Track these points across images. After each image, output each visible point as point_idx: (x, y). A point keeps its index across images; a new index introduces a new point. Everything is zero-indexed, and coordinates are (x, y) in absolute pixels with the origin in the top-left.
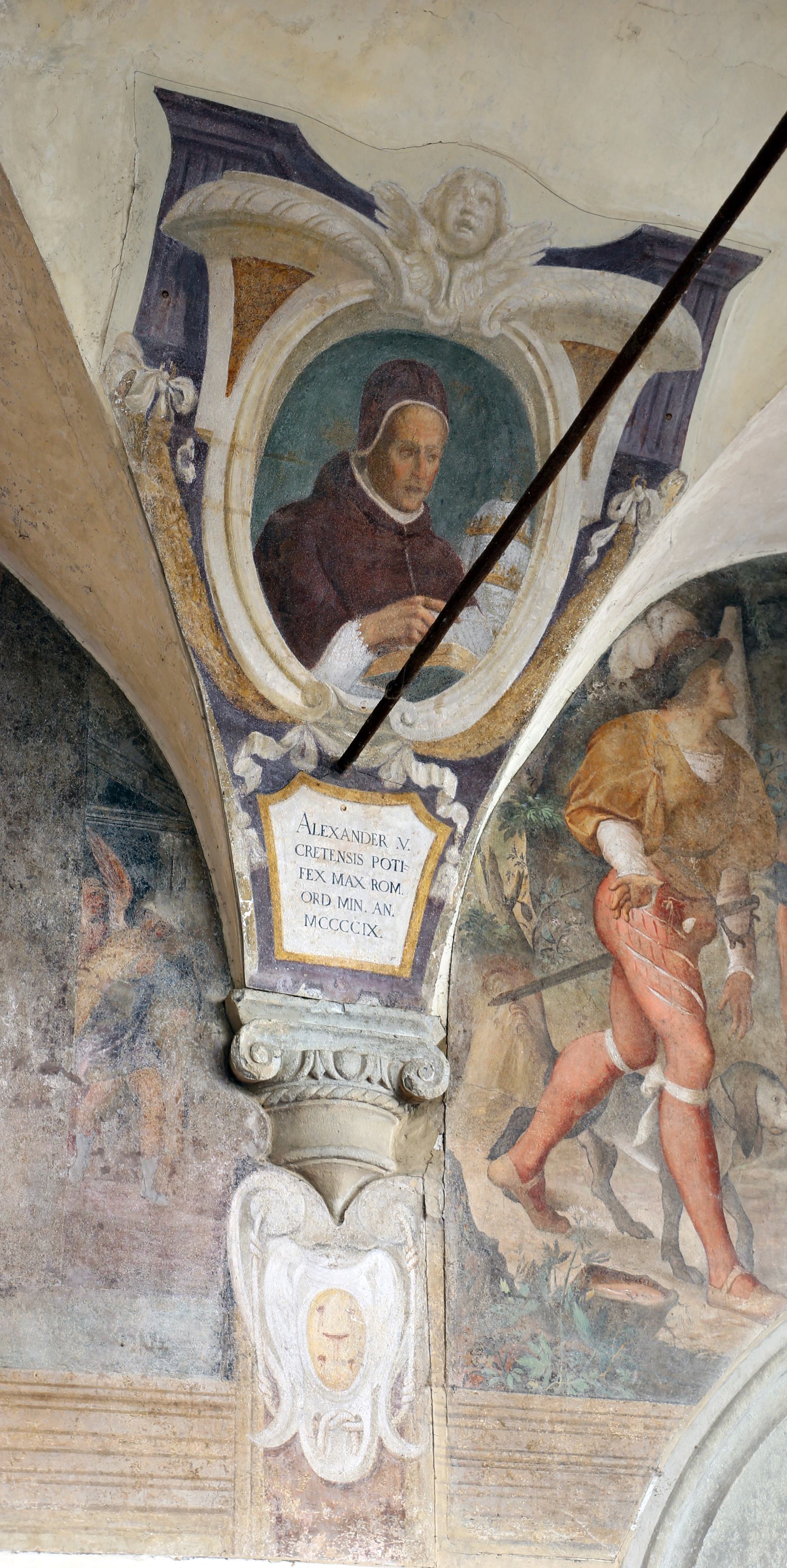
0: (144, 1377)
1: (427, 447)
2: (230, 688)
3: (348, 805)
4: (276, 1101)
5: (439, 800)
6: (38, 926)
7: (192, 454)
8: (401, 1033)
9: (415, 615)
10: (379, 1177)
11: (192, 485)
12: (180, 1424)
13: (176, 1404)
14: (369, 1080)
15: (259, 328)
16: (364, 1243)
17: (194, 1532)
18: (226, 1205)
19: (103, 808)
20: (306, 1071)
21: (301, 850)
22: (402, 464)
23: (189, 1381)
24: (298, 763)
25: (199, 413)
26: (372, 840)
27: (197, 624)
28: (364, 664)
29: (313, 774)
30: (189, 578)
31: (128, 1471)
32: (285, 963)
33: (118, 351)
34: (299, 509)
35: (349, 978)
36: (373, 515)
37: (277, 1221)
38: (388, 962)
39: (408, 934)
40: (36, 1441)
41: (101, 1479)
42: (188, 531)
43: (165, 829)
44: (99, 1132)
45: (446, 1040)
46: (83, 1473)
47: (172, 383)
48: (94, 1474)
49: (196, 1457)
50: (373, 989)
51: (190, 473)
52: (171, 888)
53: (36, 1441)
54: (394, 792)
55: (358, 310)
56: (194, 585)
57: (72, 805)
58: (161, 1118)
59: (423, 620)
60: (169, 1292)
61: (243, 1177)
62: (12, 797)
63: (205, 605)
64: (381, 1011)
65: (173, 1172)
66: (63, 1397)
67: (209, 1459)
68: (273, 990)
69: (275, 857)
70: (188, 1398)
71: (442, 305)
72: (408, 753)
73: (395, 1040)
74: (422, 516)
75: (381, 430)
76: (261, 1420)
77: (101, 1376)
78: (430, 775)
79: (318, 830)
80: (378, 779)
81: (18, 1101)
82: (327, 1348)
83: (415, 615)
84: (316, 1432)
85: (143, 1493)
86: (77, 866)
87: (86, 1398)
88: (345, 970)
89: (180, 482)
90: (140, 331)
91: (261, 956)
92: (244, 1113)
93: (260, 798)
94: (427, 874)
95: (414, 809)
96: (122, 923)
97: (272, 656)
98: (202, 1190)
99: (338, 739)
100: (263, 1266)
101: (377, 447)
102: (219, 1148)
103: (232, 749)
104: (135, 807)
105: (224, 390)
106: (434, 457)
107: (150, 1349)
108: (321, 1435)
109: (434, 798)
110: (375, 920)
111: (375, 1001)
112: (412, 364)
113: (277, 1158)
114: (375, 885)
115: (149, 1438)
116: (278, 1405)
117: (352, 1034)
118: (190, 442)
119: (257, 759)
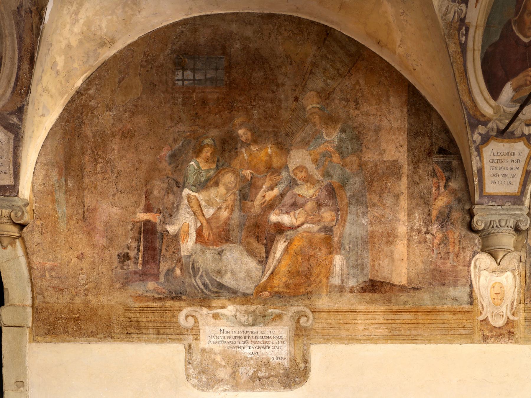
4: (483, 235)
8: (517, 212)
12: (460, 316)
13: (459, 311)
14: (507, 227)
20: (491, 226)
23: (462, 306)
28: (511, 96)
31: (449, 327)
32: (486, 196)
35: (503, 198)
38: (514, 192)
39: (520, 182)
40: (429, 321)
41: (443, 329)
43: (454, 159)
44: (439, 248)
45: (529, 212)
49: (464, 323)
50: (510, 200)
53: (429, 321)
57: (429, 156)
58: (454, 243)
61: (474, 256)
62: (414, 156)
64: (512, 207)
65: (457, 256)
66: (434, 312)
67: (467, 323)
70: (462, 310)
73: (515, 215)
76: (479, 314)
77: (442, 306)
79: (496, 154)
81: (420, 242)
84: (492, 316)
85: (453, 331)
86: (431, 175)
87: (439, 311)
88: (502, 196)
92: (475, 239)
94: (526, 163)
95: (524, 142)
96: (443, 190)
99: (503, 123)
102: (469, 249)
103: (473, 132)
104: (446, 154)
107: (453, 299)
108: (493, 316)
110: (511, 179)
111: (510, 204)
113: (483, 250)
115: (454, 319)
116: (483, 310)
117: (503, 214)
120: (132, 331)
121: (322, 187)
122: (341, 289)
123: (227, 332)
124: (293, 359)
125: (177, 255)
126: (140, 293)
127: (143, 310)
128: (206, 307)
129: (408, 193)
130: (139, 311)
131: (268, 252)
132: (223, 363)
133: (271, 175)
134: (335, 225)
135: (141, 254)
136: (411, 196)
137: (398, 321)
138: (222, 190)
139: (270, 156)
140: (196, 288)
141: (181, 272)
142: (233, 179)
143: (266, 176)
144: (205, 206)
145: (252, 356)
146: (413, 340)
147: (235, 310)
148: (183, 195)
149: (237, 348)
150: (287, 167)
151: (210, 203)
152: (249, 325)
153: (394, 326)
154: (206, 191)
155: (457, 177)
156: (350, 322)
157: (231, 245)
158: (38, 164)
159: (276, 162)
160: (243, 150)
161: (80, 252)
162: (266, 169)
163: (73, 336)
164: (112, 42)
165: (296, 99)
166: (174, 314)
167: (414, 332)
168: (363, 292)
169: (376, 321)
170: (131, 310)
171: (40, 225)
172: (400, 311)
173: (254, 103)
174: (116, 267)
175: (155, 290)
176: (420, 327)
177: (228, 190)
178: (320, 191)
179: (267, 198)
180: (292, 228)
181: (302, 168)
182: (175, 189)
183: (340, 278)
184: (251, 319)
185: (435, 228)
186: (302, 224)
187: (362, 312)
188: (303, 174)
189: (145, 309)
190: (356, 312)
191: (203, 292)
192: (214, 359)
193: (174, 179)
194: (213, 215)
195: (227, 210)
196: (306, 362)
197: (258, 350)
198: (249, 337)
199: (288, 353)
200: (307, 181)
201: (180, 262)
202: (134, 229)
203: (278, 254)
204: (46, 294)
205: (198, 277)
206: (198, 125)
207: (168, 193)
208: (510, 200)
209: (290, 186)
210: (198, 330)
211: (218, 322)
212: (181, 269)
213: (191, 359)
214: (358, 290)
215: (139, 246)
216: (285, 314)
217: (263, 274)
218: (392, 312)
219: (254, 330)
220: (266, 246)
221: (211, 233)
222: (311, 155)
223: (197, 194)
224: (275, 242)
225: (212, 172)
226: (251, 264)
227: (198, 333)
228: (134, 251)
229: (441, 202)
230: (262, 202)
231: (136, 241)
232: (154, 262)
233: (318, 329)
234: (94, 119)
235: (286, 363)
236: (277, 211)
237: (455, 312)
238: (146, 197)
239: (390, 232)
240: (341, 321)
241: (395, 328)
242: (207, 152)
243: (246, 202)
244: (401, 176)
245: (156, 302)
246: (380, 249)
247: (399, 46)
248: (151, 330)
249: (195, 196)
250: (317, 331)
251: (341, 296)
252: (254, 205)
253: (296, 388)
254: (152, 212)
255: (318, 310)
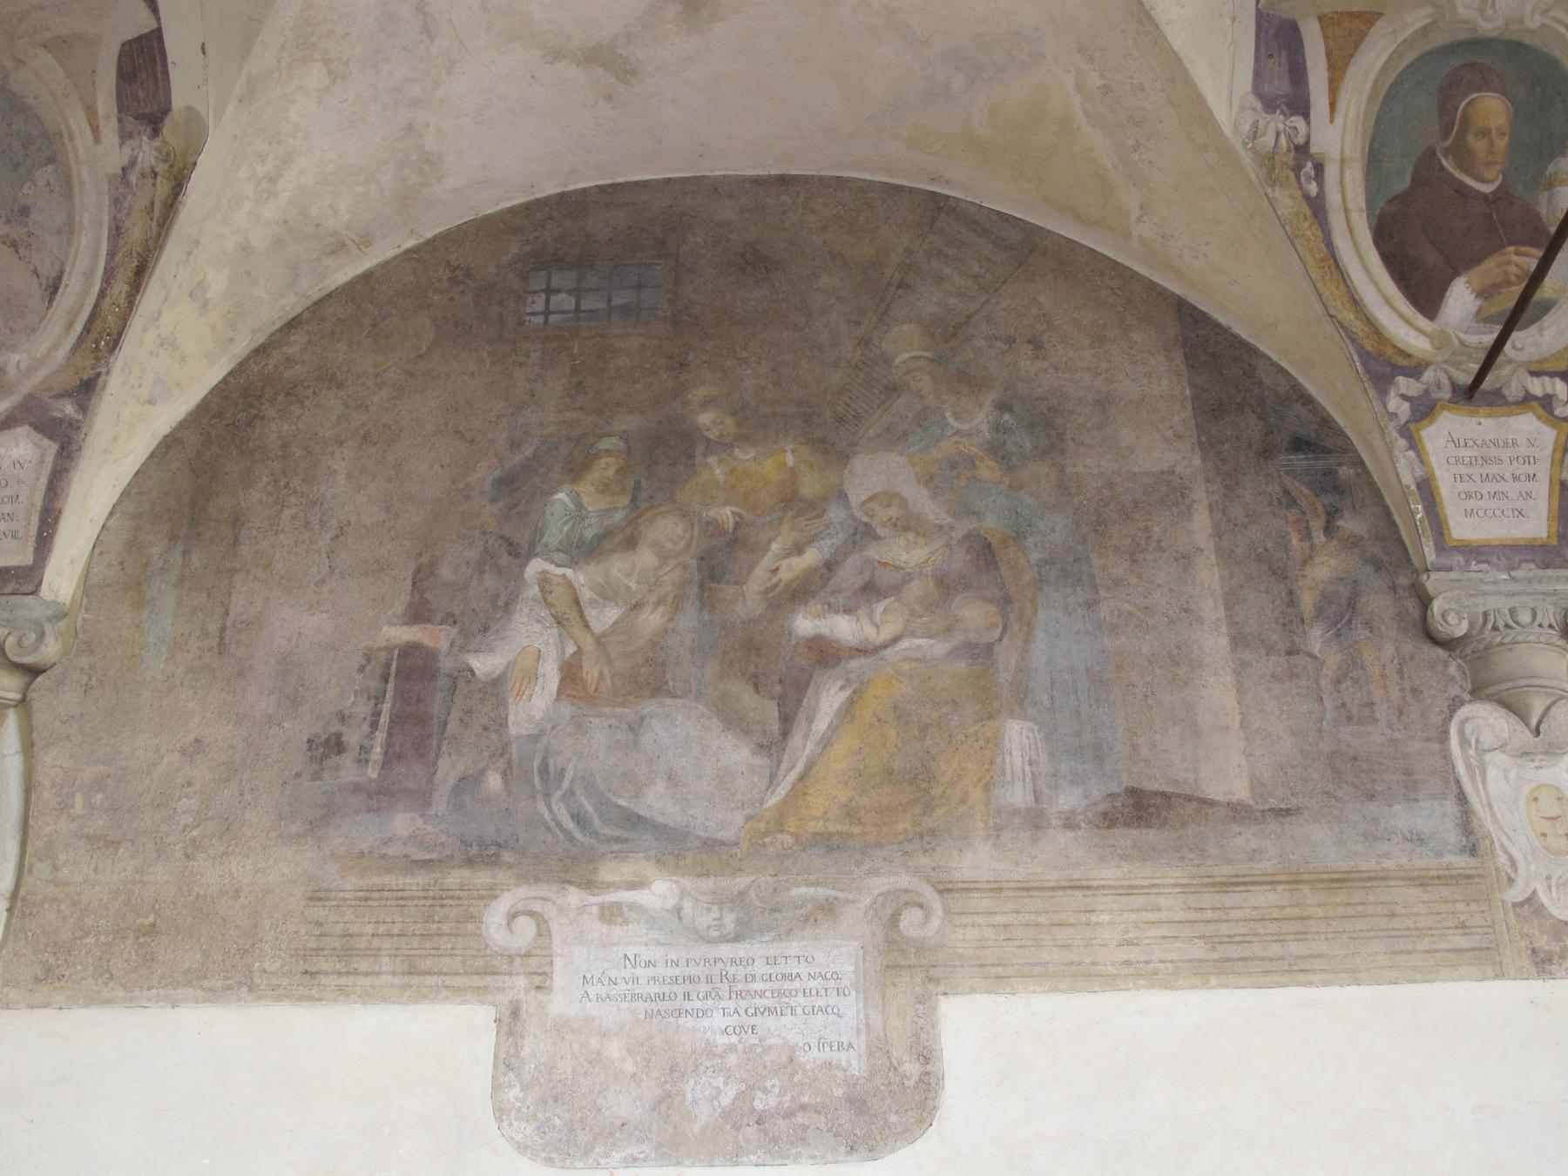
0: (1410, 861)
1: (1497, 128)
2: (1373, 346)
3: (1482, 420)
4: (1469, 652)
5: (1555, 404)
6: (1261, 550)
7: (1312, 173)
9: (1509, 263)
10: (1561, 698)
11: (1316, 198)
12: (1444, 891)
13: (1439, 877)
14: (1540, 625)
15: (1347, 65)
16: (1560, 748)
17: (1470, 964)
18: (1446, 732)
19: (1293, 457)
20: (1490, 625)
21: (1452, 460)
22: (1478, 145)
24: (1436, 395)
25: (1312, 141)
26: (1506, 444)
27: (1339, 303)
29: (1450, 401)
30: (1326, 269)
31: (1412, 926)
33: (1243, 108)
34: (1403, 198)
35: (1508, 552)
36: (1462, 191)
37: (1488, 740)
38: (1536, 535)
39: (1549, 511)
40: (1341, 910)
41: (1393, 933)
42: (1319, 233)
43: (1340, 464)
44: (1339, 692)
46: (1380, 930)
47: (1288, 123)
48: (1388, 930)
49: (1462, 913)
50: (1529, 557)
51: (1313, 188)
52: (1354, 507)
53: (1341, 910)
54: (1517, 404)
55: (1424, 32)
56: (1331, 274)
57: (1266, 459)
58: (1384, 676)
59: (1517, 265)
60: (1417, 800)
61: (1455, 711)
62: (1222, 460)
63: (1342, 287)
64: (1540, 572)
65: (1401, 714)
68: (1450, 569)
69: (1432, 468)
70: (1446, 873)
71: (1490, 12)
72: (1522, 372)
74: (1501, 184)
75: (1457, 122)
76: (1505, 883)
77: (1378, 863)
78: (1543, 385)
79: (1462, 444)
80: (1504, 397)
82: (1546, 827)
83: (1509, 263)
84: (1550, 888)
86: (1280, 503)
87: (1370, 879)
88: (1505, 547)
89: (1306, 197)
90: (1257, 90)
91: (1436, 546)
93: (1412, 426)
94: (1556, 463)
95: (1536, 414)
96: (1323, 539)
97: (1402, 316)
98: (1425, 724)
100: (1484, 773)
101: (1456, 137)
104: (1314, 452)
105: (1328, 120)
106: (1503, 134)
107: (1411, 841)
108: (1553, 889)
109: (1550, 403)
110: (1520, 505)
111: (1532, 566)
112: (1473, 65)
113: (1478, 692)
114: (1516, 478)
115: (1423, 902)
116: (1516, 870)
117: (1520, 594)
118: (1309, 165)
119: (1405, 397)
120: (324, 965)
121: (954, 542)
122: (1035, 821)
123: (649, 963)
124: (879, 1049)
125: (494, 736)
126: (365, 847)
127: (366, 899)
128: (579, 886)
129: (1218, 549)
130: (353, 903)
131: (787, 720)
132: (629, 1067)
133: (794, 517)
134: (1000, 640)
135: (380, 736)
136: (1227, 557)
137: (1234, 914)
138: (645, 557)
139: (793, 472)
140: (549, 829)
141: (506, 782)
142: (680, 529)
143: (781, 519)
144: (592, 602)
145: (734, 1039)
146: (1295, 971)
147: (677, 892)
148: (526, 576)
149: (680, 1013)
150: (842, 496)
151: (607, 594)
152: (725, 939)
153: (1225, 929)
154: (598, 563)
155: (1358, 506)
156: (1072, 920)
157: (669, 701)
158: (114, 518)
159: (810, 486)
160: (712, 460)
161: (191, 737)
162: (782, 501)
163: (124, 986)
164: (365, 241)
165: (864, 342)
166: (471, 909)
167: (1295, 948)
168: (1109, 827)
169: (1163, 915)
170: (328, 899)
171: (87, 667)
172: (1241, 880)
173: (745, 354)
174: (298, 775)
175: (414, 839)
176: (1314, 929)
177: (664, 559)
178: (948, 551)
179: (785, 575)
180: (863, 651)
181: (889, 497)
182: (505, 560)
183: (1029, 786)
184: (729, 919)
185: (1316, 638)
186: (895, 640)
187: (1110, 887)
188: (893, 511)
189: (375, 895)
190: (1088, 888)
191: (571, 838)
192: (598, 1053)
193: (502, 537)
194: (615, 623)
195: (661, 609)
196: (926, 1055)
197: (754, 1021)
198: (724, 976)
199: (862, 1026)
200: (907, 529)
201: (502, 755)
202: (368, 668)
203: (821, 725)
204: (62, 857)
205: (558, 794)
206: (582, 408)
207: (482, 572)
208: (1529, 557)
209: (854, 543)
210: (548, 959)
211: (618, 931)
212: (504, 774)
213: (517, 1055)
214: (1090, 822)
215: (377, 714)
216: (847, 901)
217: (771, 783)
218: (1213, 885)
219: (741, 954)
220: (782, 702)
221: (606, 671)
222: (913, 465)
223: (569, 572)
224: (811, 690)
225: (619, 516)
226: (737, 754)
227: (547, 969)
228: (360, 727)
229: (1325, 568)
230: (769, 584)
231: (369, 699)
232: (421, 755)
233: (960, 945)
234: (292, 408)
235: (856, 1064)
236: (817, 607)
237: (1424, 878)
238: (414, 584)
239: (1176, 652)
240: (1042, 919)
241: (1229, 936)
242: (605, 468)
243: (718, 586)
244: (1189, 507)
245: (413, 875)
246: (1150, 701)
247: (1139, 220)
248: (386, 960)
249: (564, 576)
250: (961, 951)
251: (1034, 841)
252: (743, 593)
253: (893, 1151)
254: (428, 620)
255: (960, 885)
